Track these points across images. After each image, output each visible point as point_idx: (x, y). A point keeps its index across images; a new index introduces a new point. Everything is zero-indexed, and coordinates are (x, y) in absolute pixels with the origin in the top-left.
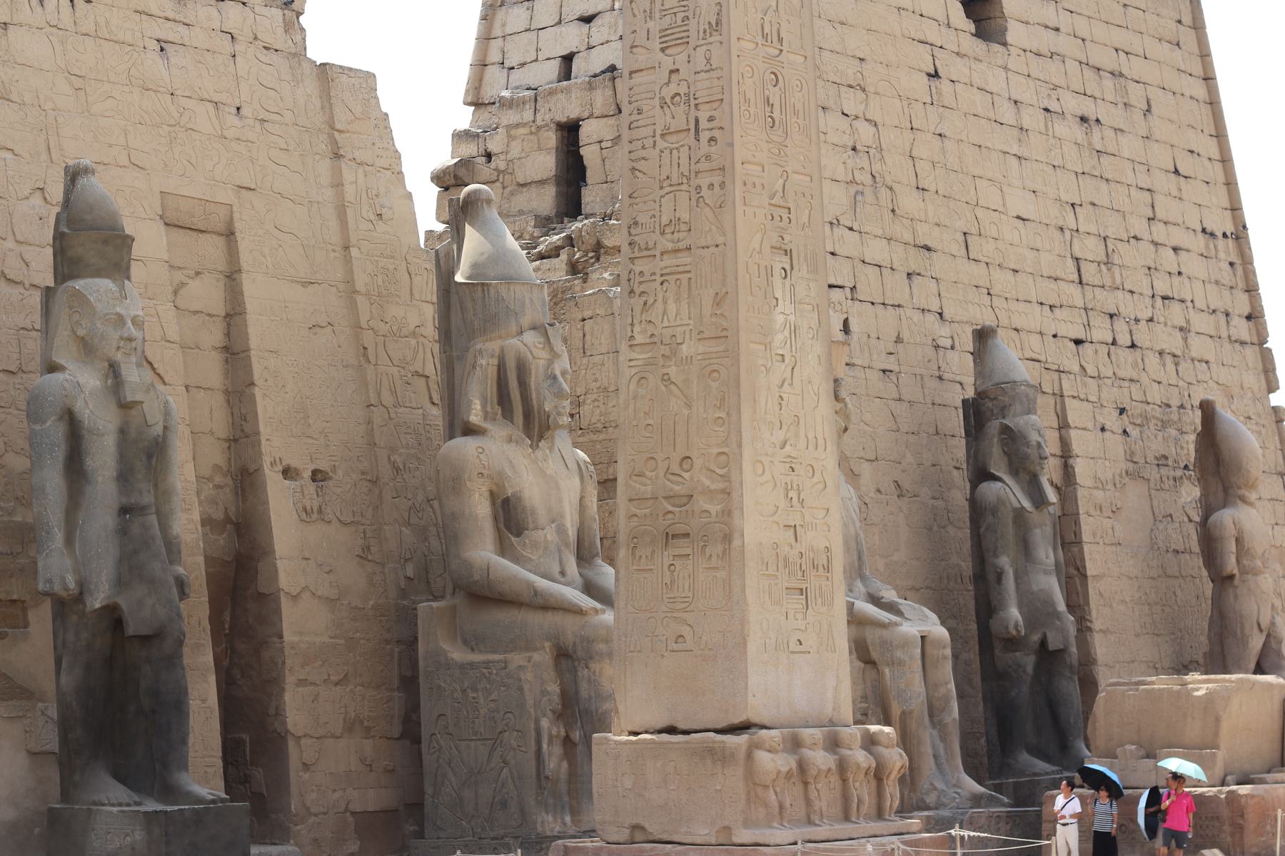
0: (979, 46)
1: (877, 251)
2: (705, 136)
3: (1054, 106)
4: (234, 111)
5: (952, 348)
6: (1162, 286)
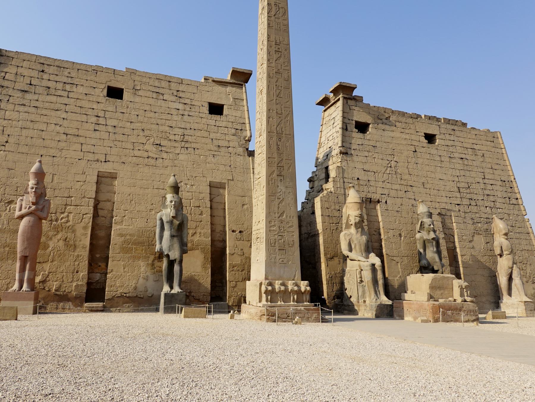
0: (430, 145)
3: (452, 156)
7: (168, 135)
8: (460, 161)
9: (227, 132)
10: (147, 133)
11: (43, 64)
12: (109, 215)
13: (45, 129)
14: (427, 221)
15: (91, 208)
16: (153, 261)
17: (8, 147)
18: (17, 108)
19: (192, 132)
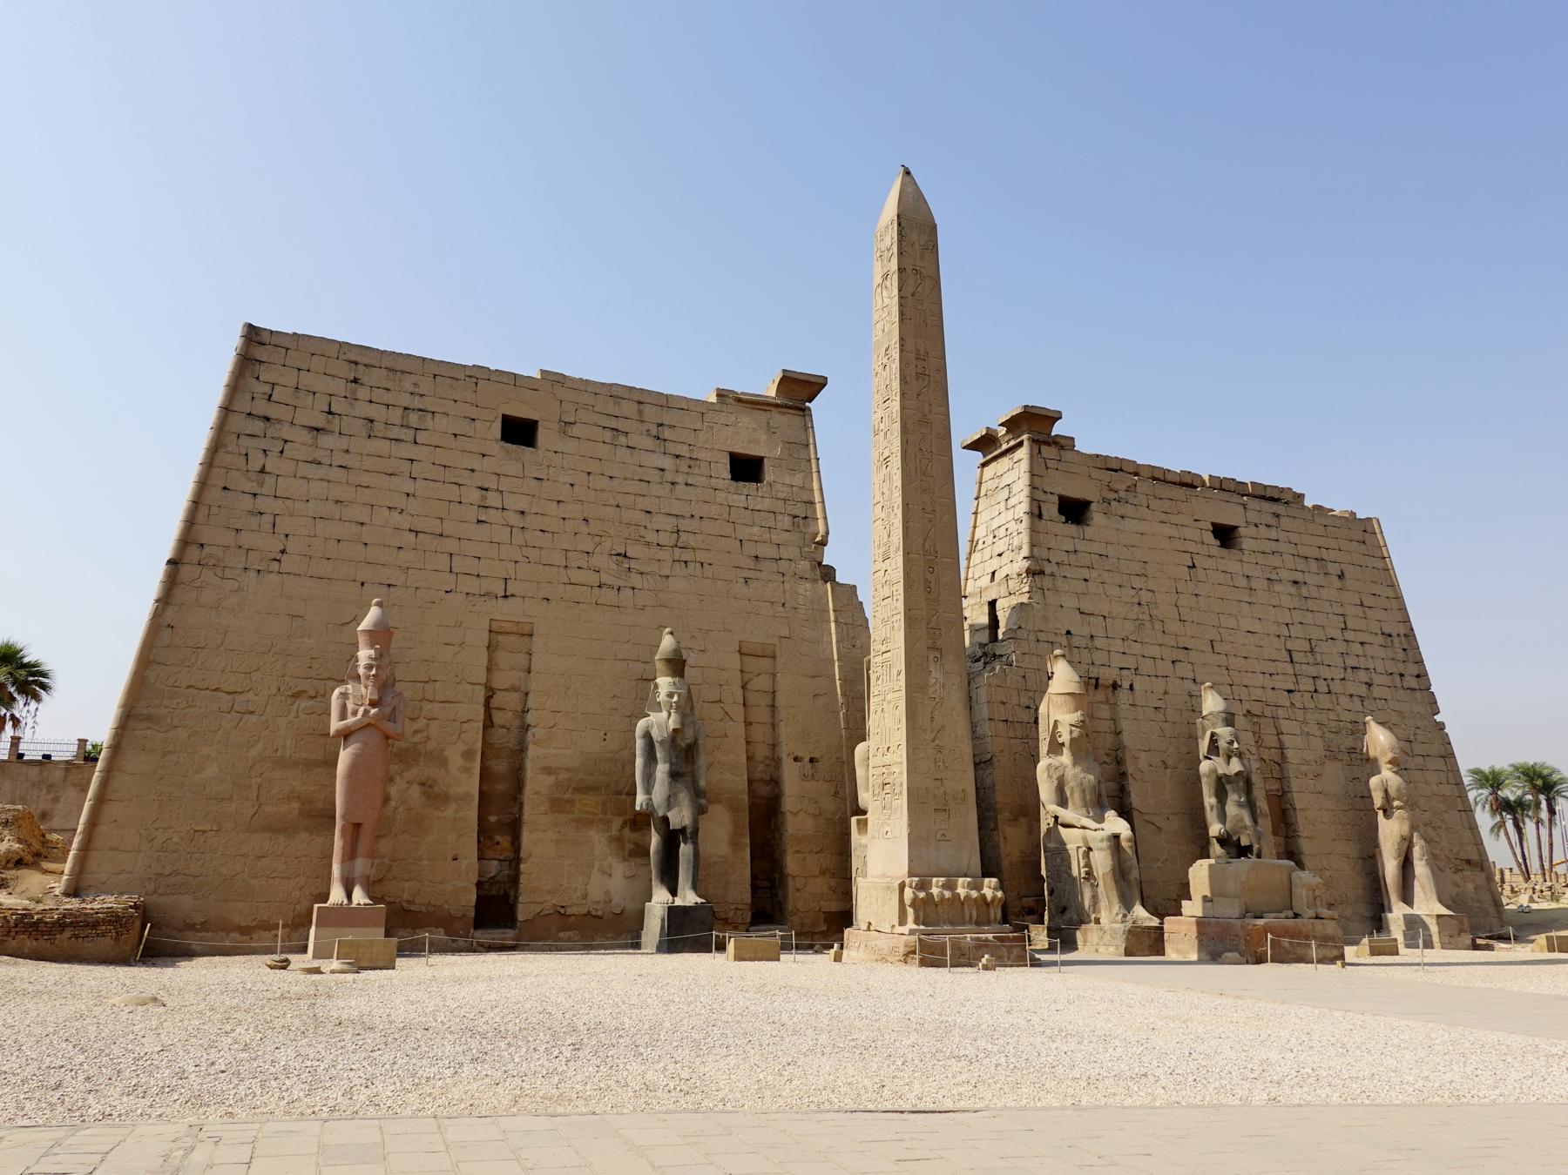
0: (1225, 552)
1: (1154, 651)
3: (1274, 577)
6: (1351, 662)
7: (643, 532)
8: (1293, 590)
10: (595, 527)
11: (357, 364)
12: (517, 723)
13: (367, 520)
14: (1224, 732)
15: (482, 710)
16: (622, 827)
17: (288, 564)
18: (305, 470)
19: (696, 521)
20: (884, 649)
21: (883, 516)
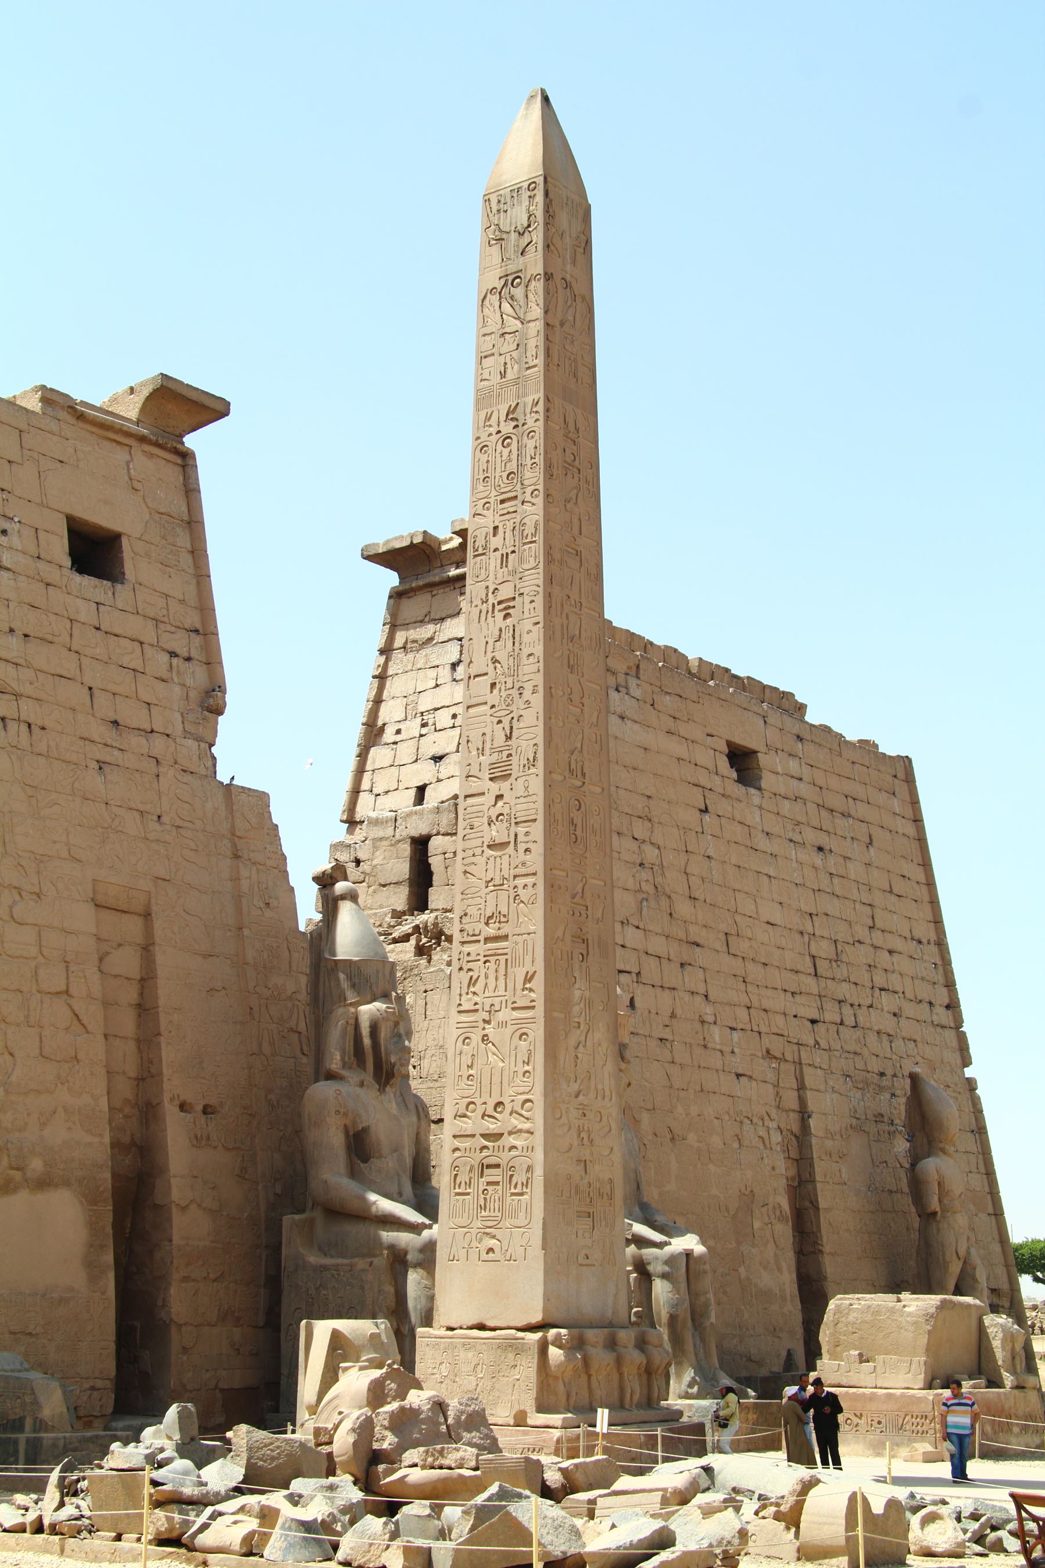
0: (739, 790)
1: (657, 945)
2: (522, 847)
3: (797, 838)
4: (155, 818)
5: (715, 1023)
6: (880, 980)
9: (137, 664)
20: (491, 931)
21: (494, 698)
